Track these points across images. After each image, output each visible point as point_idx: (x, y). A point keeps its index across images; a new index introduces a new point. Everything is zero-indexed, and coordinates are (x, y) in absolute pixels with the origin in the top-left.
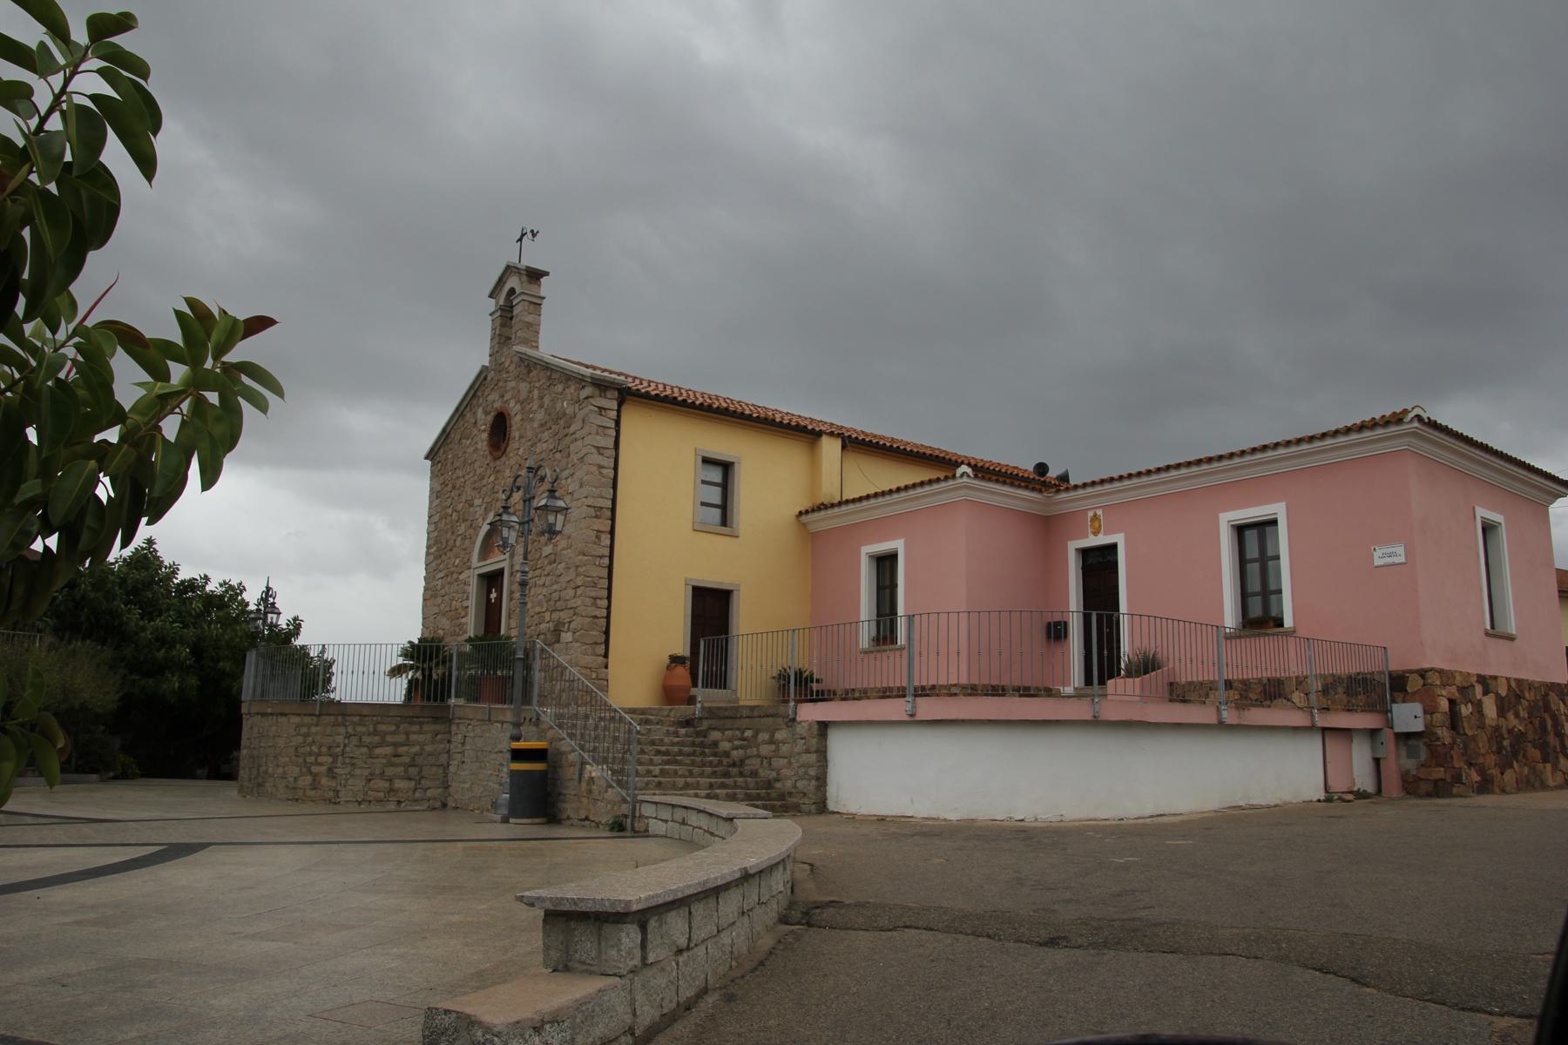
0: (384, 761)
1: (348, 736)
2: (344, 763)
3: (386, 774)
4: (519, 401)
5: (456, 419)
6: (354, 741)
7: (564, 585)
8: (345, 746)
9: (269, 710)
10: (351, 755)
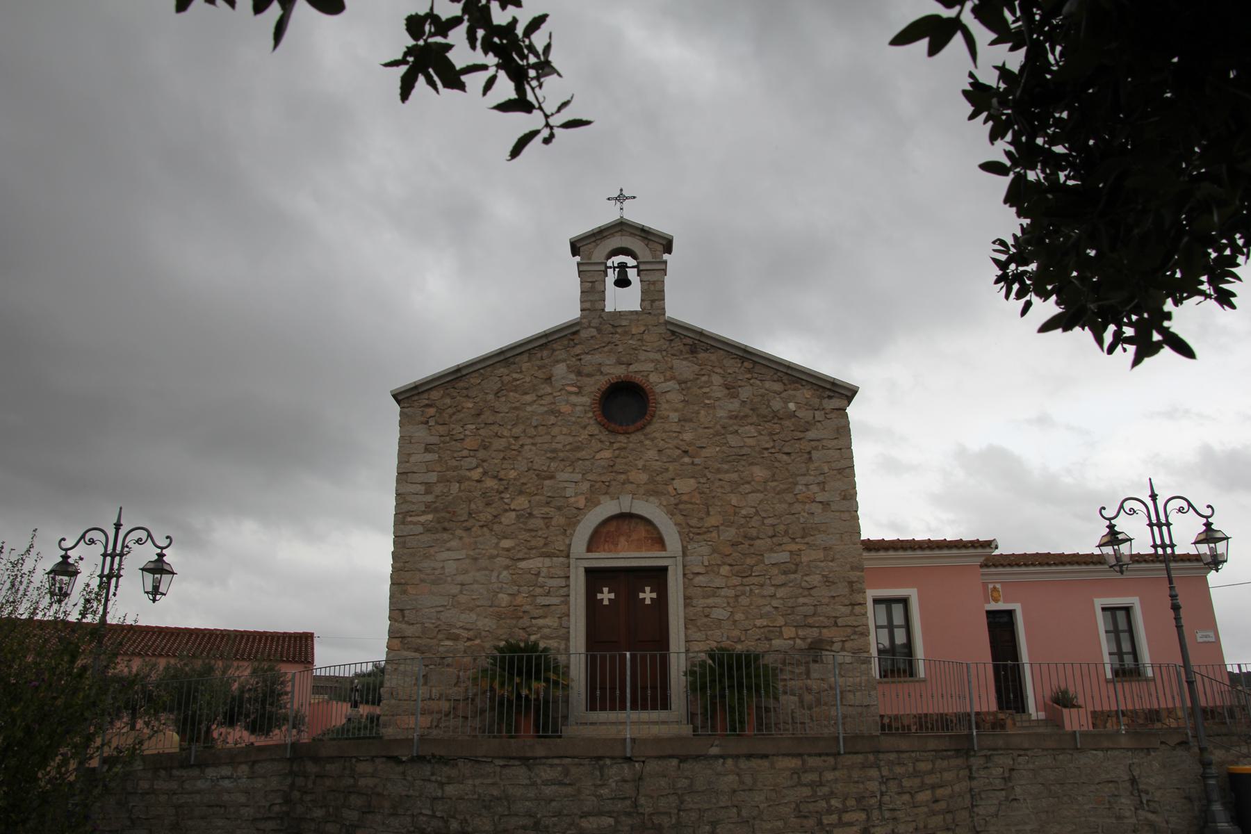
0: (926, 809)
1: (884, 781)
2: (883, 819)
3: (929, 826)
4: (673, 378)
5: (490, 362)
6: (893, 785)
7: (826, 600)
8: (882, 794)
9: (714, 751)
10: (891, 806)
